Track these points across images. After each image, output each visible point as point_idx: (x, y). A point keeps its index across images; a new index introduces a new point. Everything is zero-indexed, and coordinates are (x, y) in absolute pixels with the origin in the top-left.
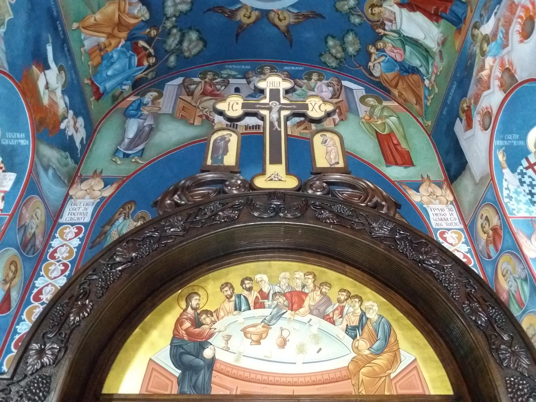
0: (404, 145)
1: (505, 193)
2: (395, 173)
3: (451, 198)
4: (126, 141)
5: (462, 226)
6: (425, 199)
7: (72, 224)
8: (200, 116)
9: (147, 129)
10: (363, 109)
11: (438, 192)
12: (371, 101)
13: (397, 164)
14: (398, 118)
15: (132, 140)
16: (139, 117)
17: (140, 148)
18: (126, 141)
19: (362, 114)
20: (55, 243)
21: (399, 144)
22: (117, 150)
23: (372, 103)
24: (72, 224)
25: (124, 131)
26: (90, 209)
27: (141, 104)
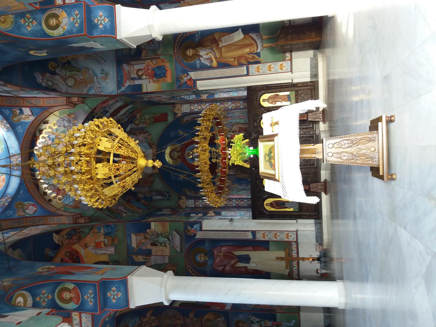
0: (159, 115)
1: (188, 98)
2: (170, 119)
3: (179, 105)
4: (163, 198)
5: (189, 105)
6: (180, 112)
7: (195, 203)
8: (150, 178)
9: (157, 193)
10: (141, 125)
11: (177, 108)
12: (137, 122)
13: (167, 118)
14: (146, 114)
15: (162, 196)
16: (152, 197)
17: (166, 193)
18: (163, 198)
19: (144, 126)
20: (201, 206)
21: (158, 116)
22: (167, 199)
23: (138, 122)
24: (195, 203)
25: (158, 200)
26: (190, 200)
27: (145, 197)
